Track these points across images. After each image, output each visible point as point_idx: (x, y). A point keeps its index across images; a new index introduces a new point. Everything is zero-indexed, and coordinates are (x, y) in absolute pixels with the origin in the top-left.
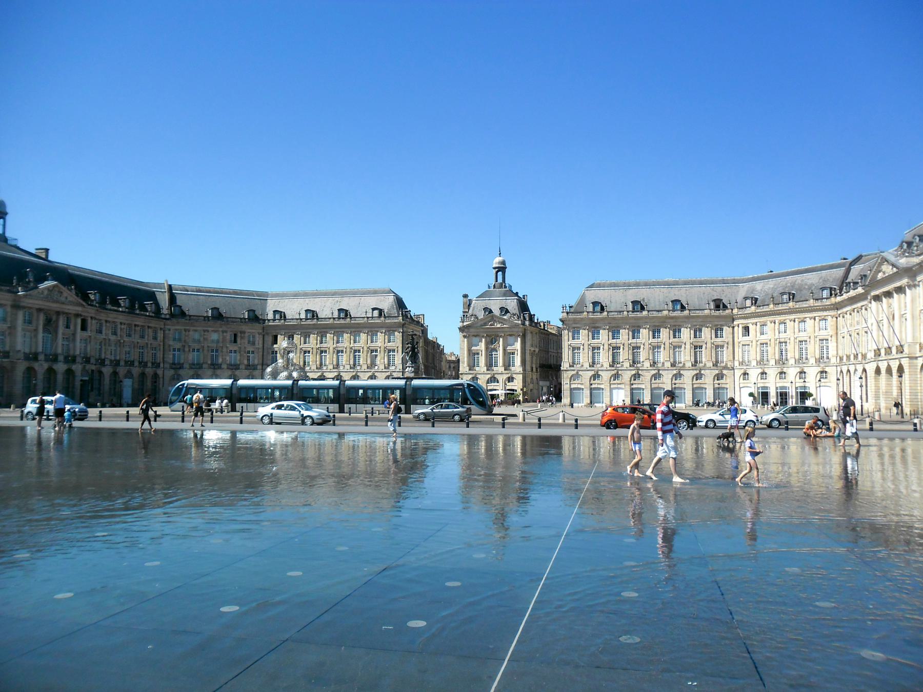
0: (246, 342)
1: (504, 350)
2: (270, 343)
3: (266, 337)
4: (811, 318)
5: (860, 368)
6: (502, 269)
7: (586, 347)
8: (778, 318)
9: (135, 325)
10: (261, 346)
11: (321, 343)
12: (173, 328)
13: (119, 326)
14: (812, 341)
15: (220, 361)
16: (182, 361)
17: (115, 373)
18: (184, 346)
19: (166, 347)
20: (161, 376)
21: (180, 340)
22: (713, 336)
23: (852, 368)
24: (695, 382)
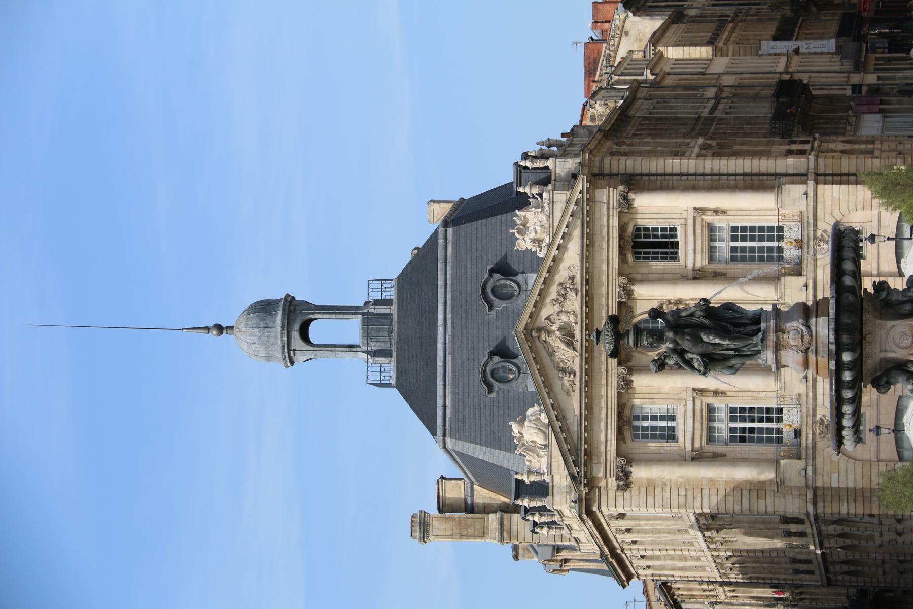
1: (698, 276)
6: (294, 318)
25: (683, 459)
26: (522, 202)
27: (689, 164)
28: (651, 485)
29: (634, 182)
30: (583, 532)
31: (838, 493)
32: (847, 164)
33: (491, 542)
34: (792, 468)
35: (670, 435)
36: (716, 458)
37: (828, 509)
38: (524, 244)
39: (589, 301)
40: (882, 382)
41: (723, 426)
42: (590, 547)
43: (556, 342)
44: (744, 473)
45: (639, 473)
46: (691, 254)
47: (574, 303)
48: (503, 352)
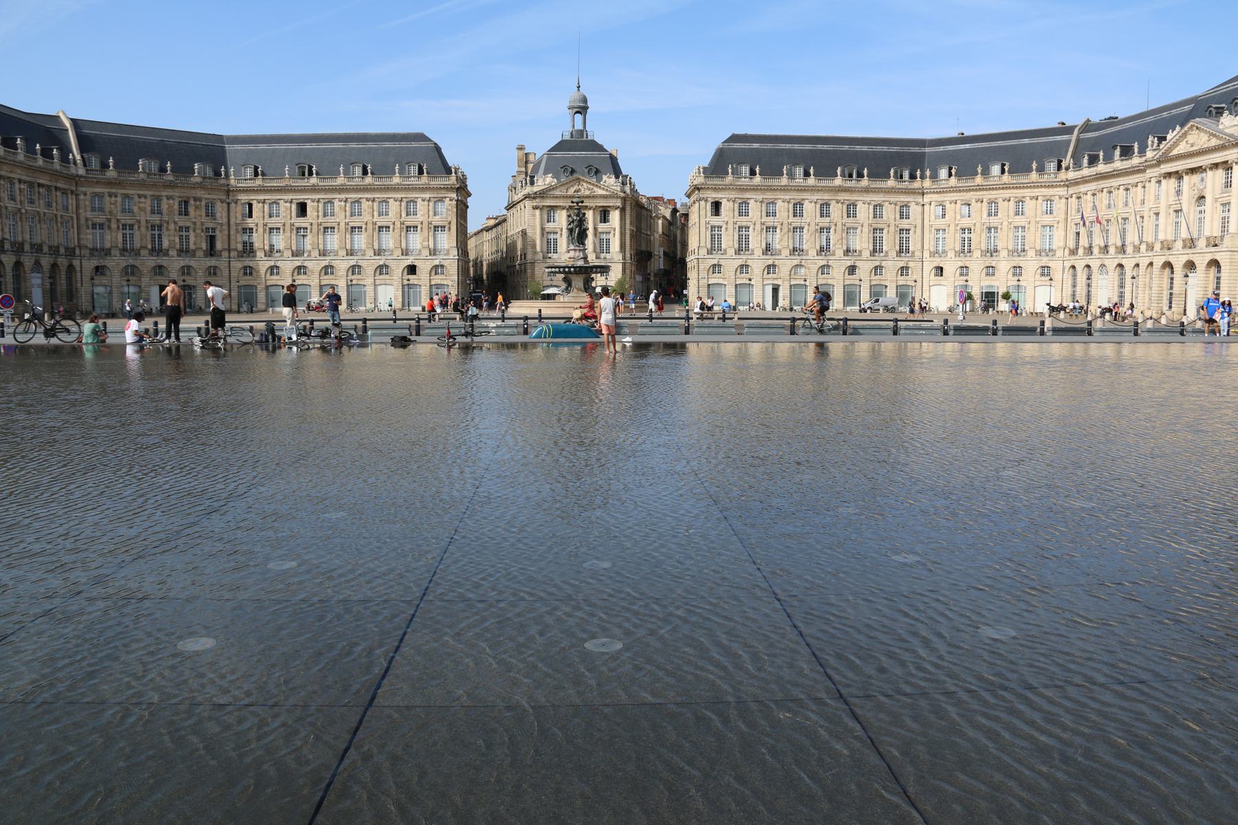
0: (203, 212)
1: (595, 229)
2: (240, 217)
3: (233, 205)
4: (1031, 198)
5: (1111, 264)
6: (582, 110)
7: (730, 226)
8: (987, 195)
9: (40, 185)
10: (225, 220)
11: (325, 215)
12: (90, 190)
13: (17, 185)
14: (1033, 229)
15: (166, 244)
16: (108, 245)
17: (18, 265)
18: (109, 220)
19: (83, 221)
20: (78, 269)
21: (101, 210)
22: (898, 216)
23: (1095, 264)
24: (873, 277)
25: (542, 225)
26: (617, 177)
27: (628, 226)
28: (534, 215)
29: (623, 210)
30: (520, 196)
31: (533, 269)
32: (628, 271)
33: (517, 169)
34: (540, 256)
35: (549, 221)
36: (543, 234)
37: (528, 266)
38: (605, 178)
39: (588, 197)
40: (565, 280)
41: (552, 236)
42: (516, 198)
43: (576, 187)
44: (538, 242)
45: (538, 212)
46: (602, 227)
47: (587, 193)
48: (573, 172)
